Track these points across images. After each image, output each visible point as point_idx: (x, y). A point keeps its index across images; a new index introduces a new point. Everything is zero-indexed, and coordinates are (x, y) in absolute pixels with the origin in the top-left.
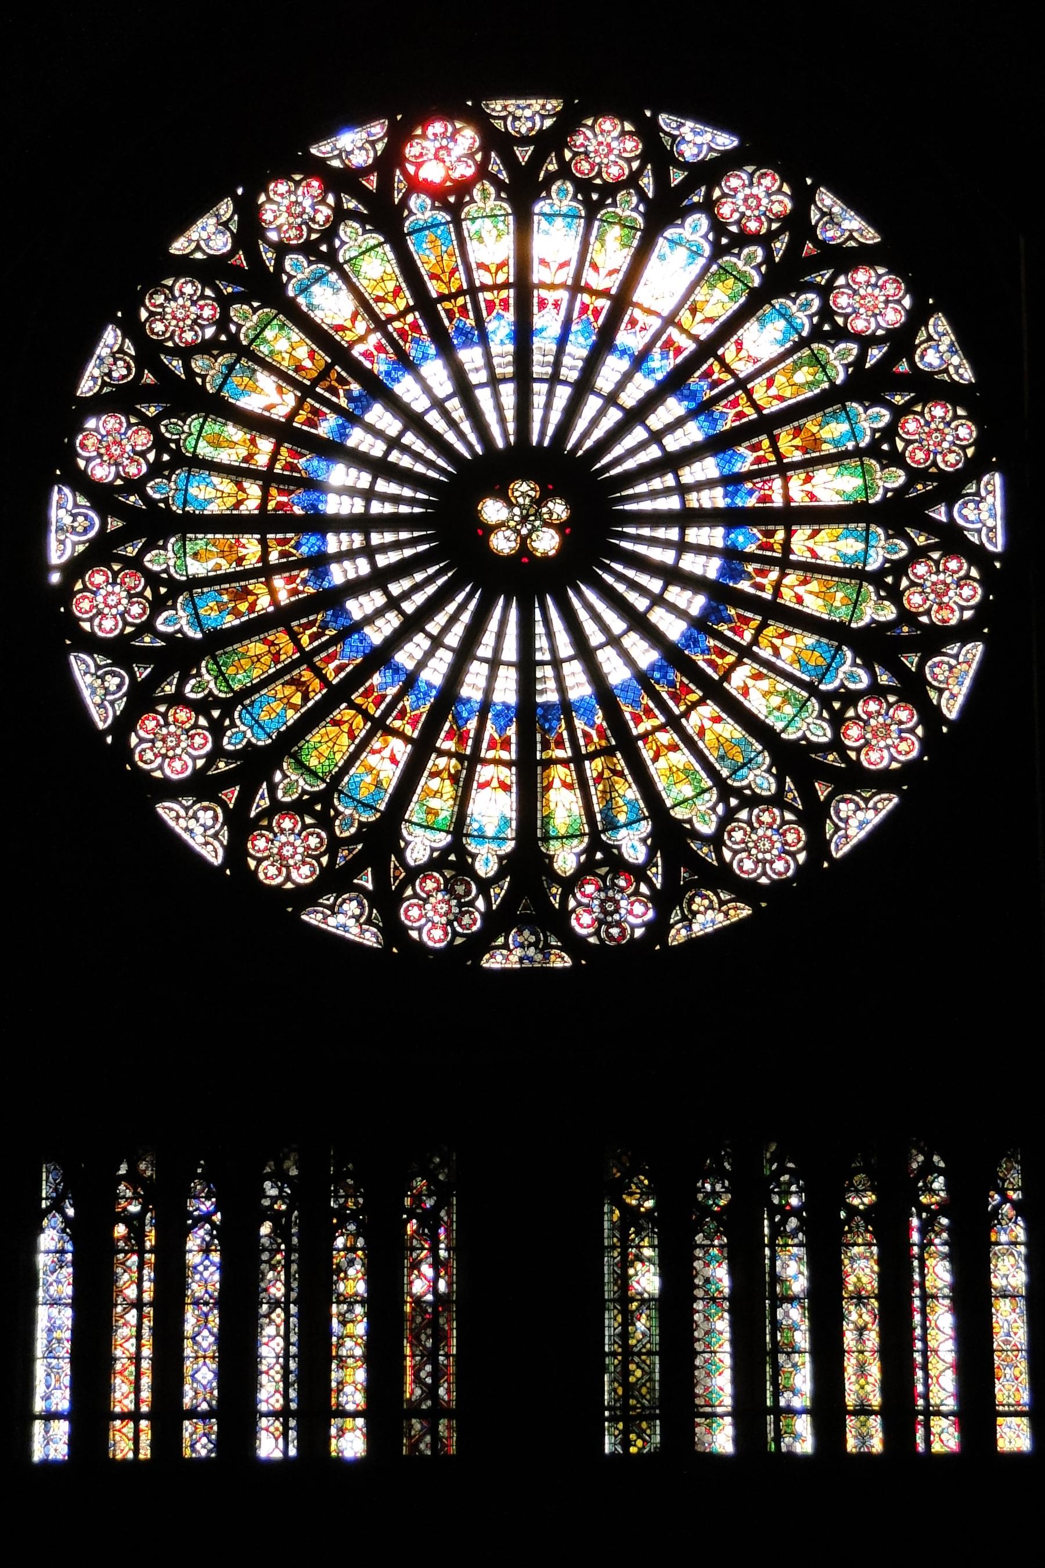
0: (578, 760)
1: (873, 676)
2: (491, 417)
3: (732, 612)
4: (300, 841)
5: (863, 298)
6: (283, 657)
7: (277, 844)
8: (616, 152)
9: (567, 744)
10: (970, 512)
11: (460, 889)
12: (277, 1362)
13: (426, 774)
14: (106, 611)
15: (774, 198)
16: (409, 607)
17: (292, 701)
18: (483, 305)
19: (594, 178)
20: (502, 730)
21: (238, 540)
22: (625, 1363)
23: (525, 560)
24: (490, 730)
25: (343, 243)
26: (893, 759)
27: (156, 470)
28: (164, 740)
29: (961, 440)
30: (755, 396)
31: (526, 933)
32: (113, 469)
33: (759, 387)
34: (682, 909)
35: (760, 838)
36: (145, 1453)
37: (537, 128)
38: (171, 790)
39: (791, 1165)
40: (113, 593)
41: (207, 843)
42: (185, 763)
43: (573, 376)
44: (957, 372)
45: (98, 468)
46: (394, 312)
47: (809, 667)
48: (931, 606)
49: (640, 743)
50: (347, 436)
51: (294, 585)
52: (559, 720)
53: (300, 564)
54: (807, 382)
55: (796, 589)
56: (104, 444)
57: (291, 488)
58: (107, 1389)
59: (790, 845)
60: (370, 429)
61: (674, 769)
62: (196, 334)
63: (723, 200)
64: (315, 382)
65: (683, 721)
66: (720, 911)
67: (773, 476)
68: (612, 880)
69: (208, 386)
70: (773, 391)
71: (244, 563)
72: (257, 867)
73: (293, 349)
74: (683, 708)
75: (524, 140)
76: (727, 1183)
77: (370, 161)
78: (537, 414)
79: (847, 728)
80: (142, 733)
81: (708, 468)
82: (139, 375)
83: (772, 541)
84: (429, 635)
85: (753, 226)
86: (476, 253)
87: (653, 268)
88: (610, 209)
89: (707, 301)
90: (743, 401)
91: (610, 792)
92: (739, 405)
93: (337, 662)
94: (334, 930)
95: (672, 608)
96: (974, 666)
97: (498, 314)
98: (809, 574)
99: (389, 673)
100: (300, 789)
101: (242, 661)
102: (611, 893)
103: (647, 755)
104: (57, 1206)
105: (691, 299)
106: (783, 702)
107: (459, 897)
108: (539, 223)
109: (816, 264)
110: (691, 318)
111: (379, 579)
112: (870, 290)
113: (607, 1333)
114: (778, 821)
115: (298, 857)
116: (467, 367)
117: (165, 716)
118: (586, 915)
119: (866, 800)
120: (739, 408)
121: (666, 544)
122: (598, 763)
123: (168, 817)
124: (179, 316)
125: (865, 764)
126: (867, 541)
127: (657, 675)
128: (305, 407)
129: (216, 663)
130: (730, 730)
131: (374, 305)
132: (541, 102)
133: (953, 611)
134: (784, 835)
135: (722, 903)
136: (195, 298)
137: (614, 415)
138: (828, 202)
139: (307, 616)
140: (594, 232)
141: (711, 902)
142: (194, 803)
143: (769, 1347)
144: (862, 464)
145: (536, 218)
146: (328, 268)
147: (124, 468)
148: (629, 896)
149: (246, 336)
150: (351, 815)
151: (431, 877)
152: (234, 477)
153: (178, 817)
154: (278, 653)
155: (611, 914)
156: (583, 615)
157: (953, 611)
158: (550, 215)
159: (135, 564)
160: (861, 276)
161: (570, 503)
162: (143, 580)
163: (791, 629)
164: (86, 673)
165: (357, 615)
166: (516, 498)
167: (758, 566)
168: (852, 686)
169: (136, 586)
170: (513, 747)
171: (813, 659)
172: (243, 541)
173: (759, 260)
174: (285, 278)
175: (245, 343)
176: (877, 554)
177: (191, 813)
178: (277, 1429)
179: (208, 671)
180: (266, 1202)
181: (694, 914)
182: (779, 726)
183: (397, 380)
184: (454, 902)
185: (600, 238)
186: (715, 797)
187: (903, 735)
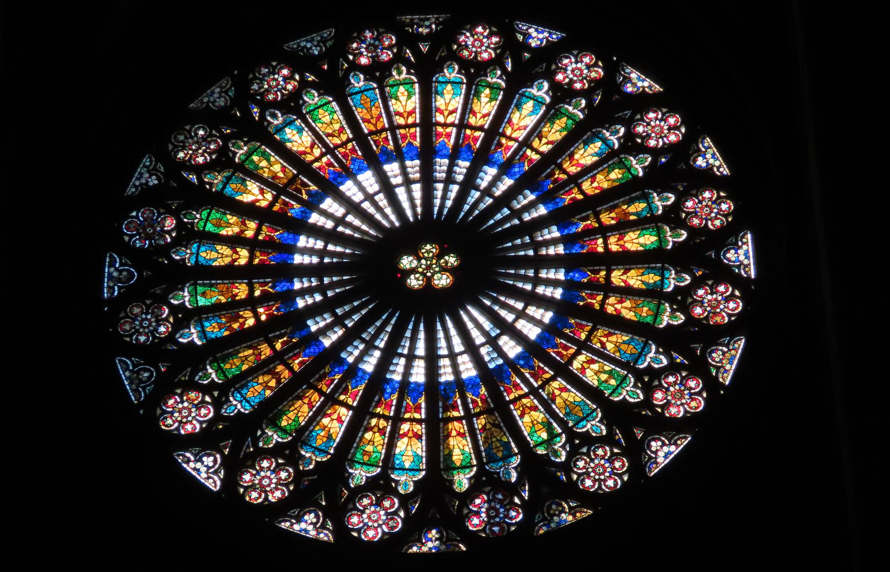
2: (406, 205)
4: (274, 475)
5: (653, 127)
7: (258, 477)
9: (461, 408)
10: (731, 255)
11: (387, 504)
13: (362, 429)
14: (141, 330)
17: (269, 384)
20: (415, 400)
28: (180, 412)
29: (724, 211)
35: (597, 465)
41: (209, 478)
42: (194, 425)
44: (718, 170)
46: (339, 142)
47: (627, 355)
49: (512, 407)
50: (309, 218)
51: (271, 311)
52: (456, 392)
54: (618, 178)
55: (616, 306)
56: (142, 227)
59: (617, 470)
60: (325, 213)
61: (535, 422)
62: (206, 158)
64: (286, 185)
68: (494, 496)
74: (540, 383)
79: (654, 393)
83: (598, 276)
85: (578, 86)
86: (395, 106)
89: (550, 132)
91: (491, 438)
92: (573, 193)
93: (301, 359)
95: (532, 320)
96: (740, 351)
97: (409, 142)
103: (516, 413)
105: (538, 130)
106: (609, 377)
107: (386, 509)
112: (658, 122)
115: (273, 486)
116: (389, 174)
120: (573, 195)
127: (522, 362)
128: (279, 201)
130: (574, 396)
131: (326, 138)
139: (279, 330)
140: (473, 92)
149: (239, 159)
150: (310, 457)
151: (366, 496)
154: (260, 354)
155: (494, 518)
156: (470, 325)
158: (443, 82)
161: (458, 255)
163: (612, 331)
166: (423, 253)
168: (656, 366)
170: (423, 411)
171: (629, 349)
173: (583, 105)
176: (670, 283)
184: (382, 513)
186: (564, 440)
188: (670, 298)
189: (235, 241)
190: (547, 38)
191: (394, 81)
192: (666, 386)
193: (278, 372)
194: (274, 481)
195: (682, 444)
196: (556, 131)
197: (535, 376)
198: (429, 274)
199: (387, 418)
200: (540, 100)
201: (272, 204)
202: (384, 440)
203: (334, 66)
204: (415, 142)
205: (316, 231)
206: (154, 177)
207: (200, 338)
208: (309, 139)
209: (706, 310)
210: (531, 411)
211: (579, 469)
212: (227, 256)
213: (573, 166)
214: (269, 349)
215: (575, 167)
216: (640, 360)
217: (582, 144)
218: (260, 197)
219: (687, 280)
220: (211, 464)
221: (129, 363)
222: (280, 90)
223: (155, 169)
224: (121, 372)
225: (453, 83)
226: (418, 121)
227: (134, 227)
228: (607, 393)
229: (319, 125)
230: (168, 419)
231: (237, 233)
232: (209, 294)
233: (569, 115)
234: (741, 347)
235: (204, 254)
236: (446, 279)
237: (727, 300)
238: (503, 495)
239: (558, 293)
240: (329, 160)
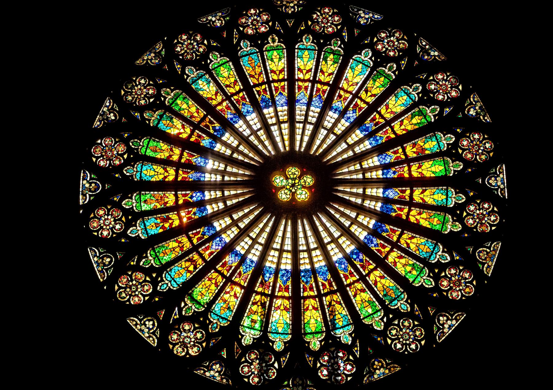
3: (388, 227)
4: (193, 335)
5: (441, 86)
9: (315, 289)
13: (251, 303)
14: (104, 227)
15: (400, 42)
16: (242, 225)
17: (189, 269)
18: (273, 88)
20: (285, 282)
21: (164, 194)
24: (279, 283)
25: (211, 61)
27: (128, 163)
28: (130, 288)
29: (487, 149)
30: (395, 129)
32: (108, 162)
35: (404, 333)
40: (108, 219)
41: (149, 337)
43: (314, 120)
44: (484, 119)
45: (101, 162)
46: (234, 92)
47: (424, 253)
48: (477, 224)
49: (348, 289)
52: (311, 278)
53: (193, 205)
55: (417, 217)
56: (104, 151)
57: (189, 171)
59: (418, 337)
61: (364, 301)
62: (146, 101)
63: (379, 43)
64: (200, 122)
65: (367, 278)
66: (387, 368)
67: (404, 165)
72: (173, 348)
73: (189, 108)
74: (367, 272)
78: (298, 138)
79: (442, 281)
80: (120, 284)
81: (374, 161)
83: (404, 195)
84: (251, 238)
85: (392, 54)
86: (271, 66)
89: (373, 87)
91: (335, 312)
92: (388, 133)
93: (209, 251)
95: (361, 225)
97: (280, 92)
98: (422, 210)
99: (233, 255)
100: (193, 310)
103: (351, 294)
105: (365, 86)
106: (412, 269)
108: (298, 53)
110: (365, 94)
111: (228, 211)
112: (444, 82)
114: (412, 326)
116: (267, 116)
117: (131, 276)
119: (452, 316)
120: (388, 135)
121: (357, 195)
122: (328, 298)
127: (355, 257)
129: (155, 251)
130: (388, 282)
131: (225, 89)
133: (487, 227)
134: (415, 332)
137: (332, 137)
138: (424, 43)
139: (196, 230)
140: (322, 57)
141: (382, 364)
144: (444, 160)
145: (296, 50)
146: (205, 72)
147: (113, 162)
149: (168, 102)
151: (253, 352)
152: (163, 166)
153: (136, 324)
154: (183, 246)
157: (487, 227)
158: (302, 49)
159: (118, 206)
160: (440, 77)
163: (414, 235)
164: (94, 257)
166: (289, 175)
167: (399, 206)
168: (443, 262)
169: (118, 216)
172: (167, 195)
177: (142, 322)
179: (151, 255)
185: (325, 59)
189: (166, 163)
190: (371, 18)
191: (270, 47)
192: (449, 276)
193: (195, 260)
195: (460, 319)
196: (377, 87)
197: (363, 267)
198: (293, 190)
200: (366, 64)
201: (190, 136)
202: (265, 311)
204: (284, 93)
208: (214, 89)
209: (475, 221)
210: (361, 292)
213: (388, 113)
214: (189, 243)
216: (432, 257)
217: (394, 97)
218: (182, 131)
219: (463, 199)
221: (97, 251)
222: (194, 52)
224: (92, 258)
226: (286, 77)
227: (99, 151)
228: (411, 280)
229: (221, 79)
230: (123, 293)
231: (167, 157)
232: (149, 202)
233: (386, 76)
234: (499, 249)
235: (145, 172)
236: (305, 194)
237: (489, 214)
238: (343, 354)
239: (378, 206)
240: (227, 104)
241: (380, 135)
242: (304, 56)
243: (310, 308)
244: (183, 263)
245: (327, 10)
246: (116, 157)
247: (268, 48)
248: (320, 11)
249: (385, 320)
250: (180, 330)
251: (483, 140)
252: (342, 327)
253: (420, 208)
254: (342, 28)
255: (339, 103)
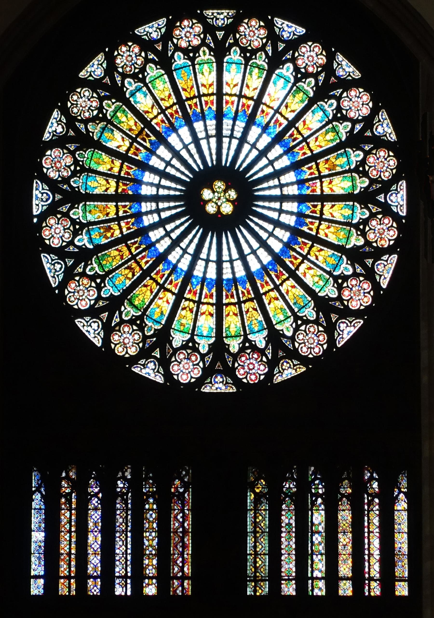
0: (239, 303)
1: (354, 269)
5: (354, 102)
6: (124, 257)
8: (257, 35)
12: (123, 556)
13: (180, 308)
15: (319, 57)
17: (128, 276)
19: (248, 46)
20: (210, 290)
21: (107, 205)
22: (255, 558)
23: (219, 216)
24: (205, 290)
25: (148, 74)
26: (361, 305)
27: (74, 174)
30: (310, 145)
31: (219, 377)
33: (311, 140)
34: (279, 368)
35: (309, 338)
36: (73, 593)
37: (226, 23)
38: (81, 314)
39: (319, 476)
40: (58, 228)
41: (95, 337)
45: (51, 173)
52: (232, 286)
53: (131, 216)
57: (128, 183)
58: (58, 567)
61: (277, 308)
64: (137, 136)
66: (293, 369)
69: (95, 137)
70: (317, 143)
71: (109, 215)
74: (280, 281)
75: (220, 29)
76: (295, 484)
77: (159, 37)
80: (69, 289)
81: (290, 177)
82: (67, 132)
86: (201, 79)
87: (271, 88)
88: (254, 61)
90: (306, 147)
94: (144, 375)
96: (394, 265)
98: (330, 224)
99: (166, 264)
101: (109, 259)
102: (251, 361)
103: (266, 302)
104: (38, 490)
107: (193, 362)
109: (335, 87)
113: (248, 546)
114: (316, 331)
115: (131, 344)
117: (78, 281)
118: (242, 370)
119: (351, 322)
123: (80, 325)
124: (83, 106)
125: (350, 307)
126: (353, 210)
127: (270, 267)
130: (299, 291)
132: (227, 11)
134: (318, 337)
135: (294, 365)
136: (89, 98)
140: (248, 71)
141: (290, 365)
142: (90, 320)
143: (310, 552)
145: (225, 64)
148: (259, 362)
149: (110, 115)
153: (84, 326)
155: (252, 370)
159: (66, 215)
160: (353, 93)
162: (69, 222)
165: (153, 239)
167: (310, 220)
172: (109, 206)
174: (125, 89)
175: (109, 118)
177: (89, 324)
178: (123, 584)
179: (95, 262)
180: (119, 490)
181: (284, 370)
182: (317, 291)
183: (169, 136)
185: (251, 74)
186: (292, 320)
187: (366, 295)
188: (356, 226)
194: (131, 341)
199: (194, 302)
200: (287, 79)
203: (165, 47)
205: (154, 170)
206: (60, 126)
207: (89, 242)
211: (300, 340)
212: (103, 185)
215: (306, 130)
220: (96, 328)
223: (60, 120)
225: (236, 63)
229: (157, 92)
241: (297, 151)
242: (231, 70)
243: (231, 313)
244: (123, 270)
245: (253, 23)
246: (64, 168)
247: (200, 62)
248: (247, 24)
249: (294, 325)
250: (120, 332)
251: (388, 157)
252: (258, 332)
253: (329, 223)
254: (267, 42)
255: (262, 118)
